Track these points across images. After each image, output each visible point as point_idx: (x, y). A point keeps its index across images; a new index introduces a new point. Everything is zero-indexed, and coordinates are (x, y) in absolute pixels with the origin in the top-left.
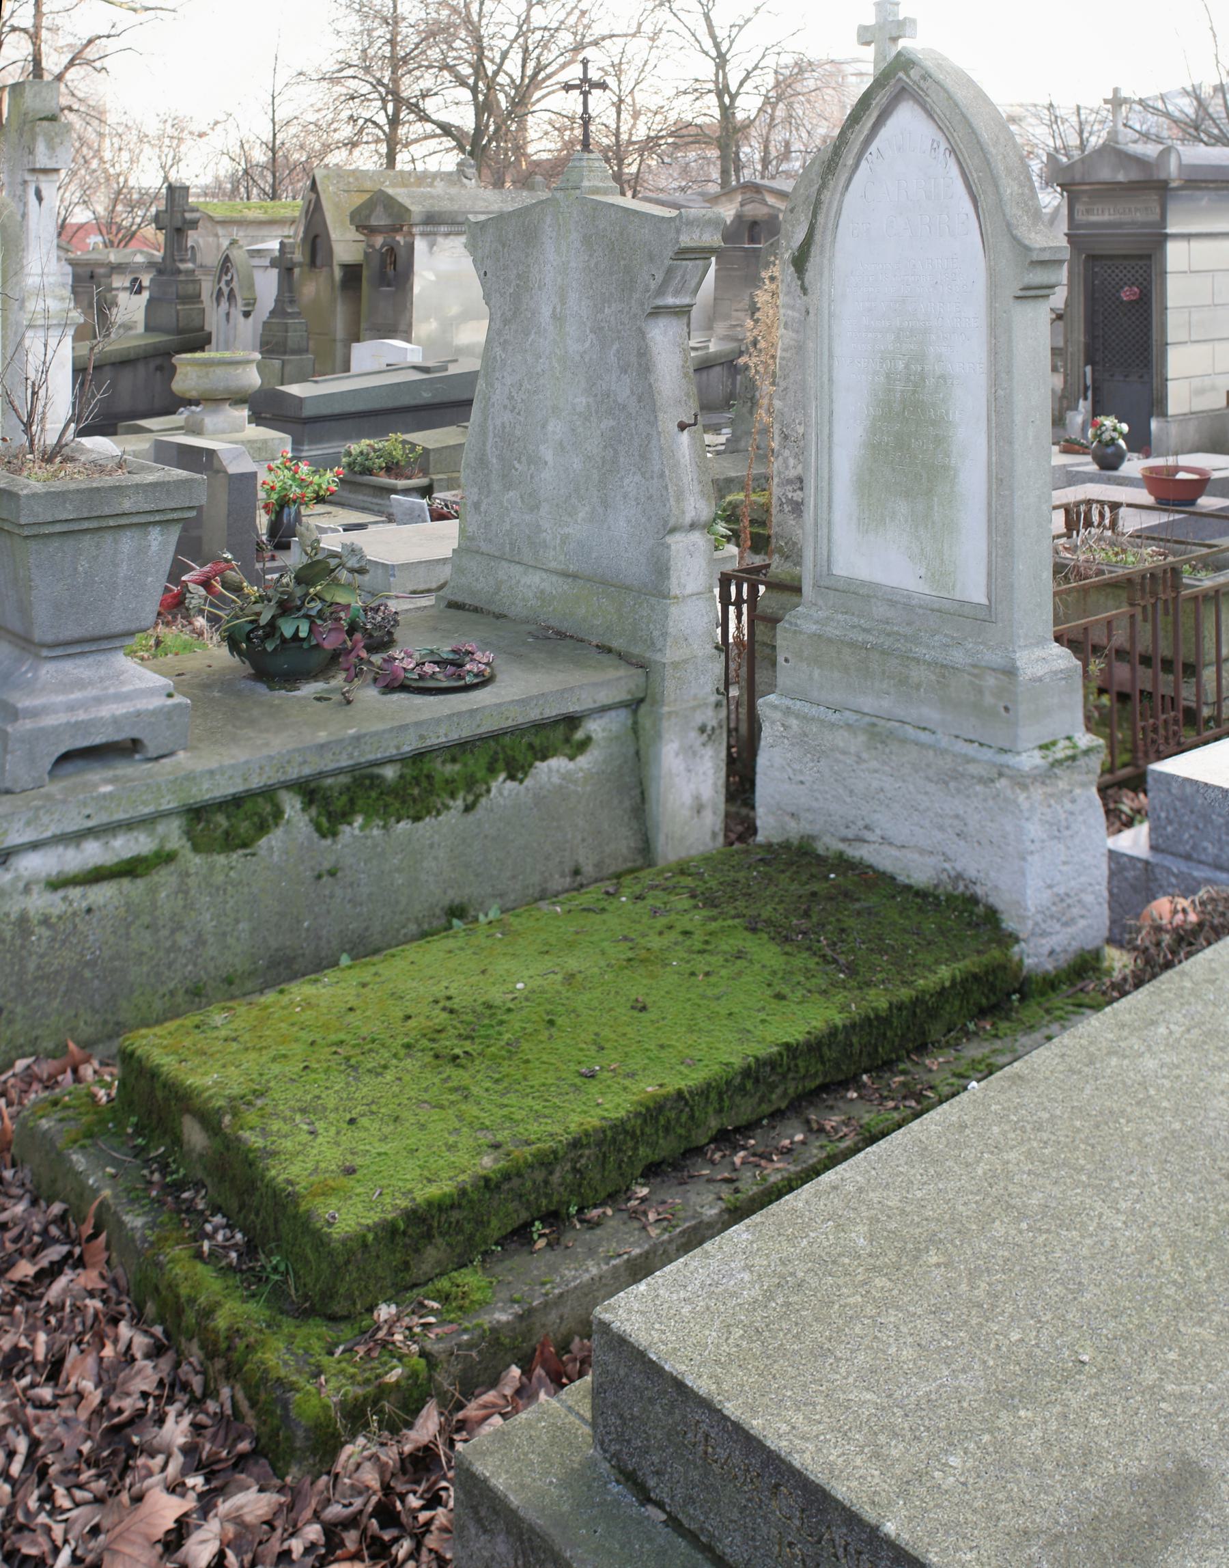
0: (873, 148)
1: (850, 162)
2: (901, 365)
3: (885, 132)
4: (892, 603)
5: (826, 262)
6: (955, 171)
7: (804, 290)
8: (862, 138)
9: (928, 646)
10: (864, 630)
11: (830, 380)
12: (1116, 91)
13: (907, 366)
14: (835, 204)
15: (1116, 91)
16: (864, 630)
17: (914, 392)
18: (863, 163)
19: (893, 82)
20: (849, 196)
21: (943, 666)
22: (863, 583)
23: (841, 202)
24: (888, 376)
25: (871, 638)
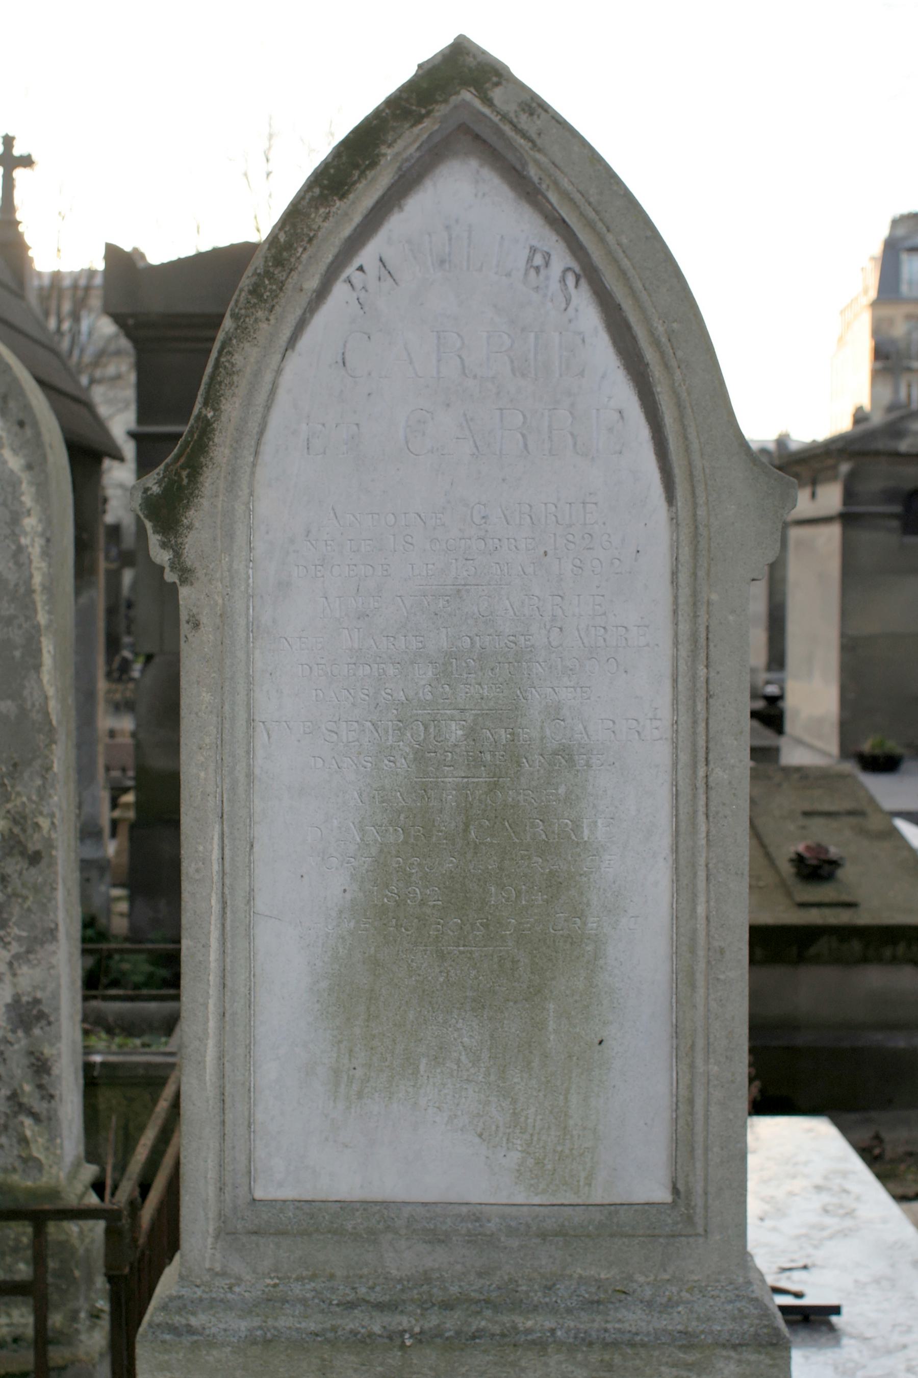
0: (367, 255)
1: (312, 284)
2: (455, 732)
3: (397, 225)
4: (436, 1237)
5: (240, 508)
6: (588, 316)
7: (636, 560)
8: (347, 231)
9: (553, 1310)
10: (380, 1307)
11: (250, 775)
12: (27, 161)
13: (472, 733)
14: (268, 377)
15: (27, 161)
16: (380, 1307)
17: (494, 787)
18: (340, 290)
19: (441, 110)
20: (295, 363)
21: (606, 1345)
22: (346, 1207)
23: (279, 371)
24: (420, 757)
25: (405, 1322)
